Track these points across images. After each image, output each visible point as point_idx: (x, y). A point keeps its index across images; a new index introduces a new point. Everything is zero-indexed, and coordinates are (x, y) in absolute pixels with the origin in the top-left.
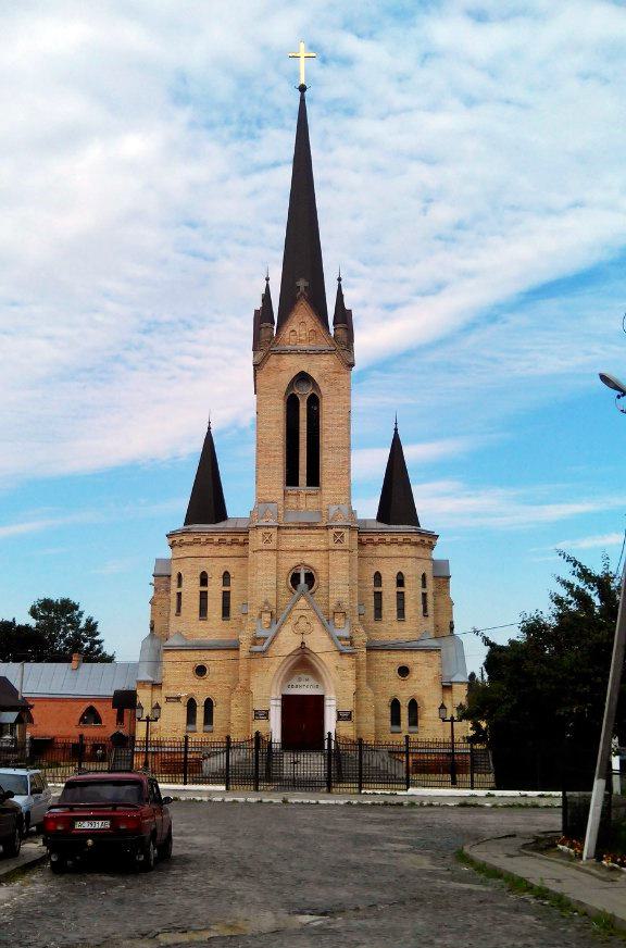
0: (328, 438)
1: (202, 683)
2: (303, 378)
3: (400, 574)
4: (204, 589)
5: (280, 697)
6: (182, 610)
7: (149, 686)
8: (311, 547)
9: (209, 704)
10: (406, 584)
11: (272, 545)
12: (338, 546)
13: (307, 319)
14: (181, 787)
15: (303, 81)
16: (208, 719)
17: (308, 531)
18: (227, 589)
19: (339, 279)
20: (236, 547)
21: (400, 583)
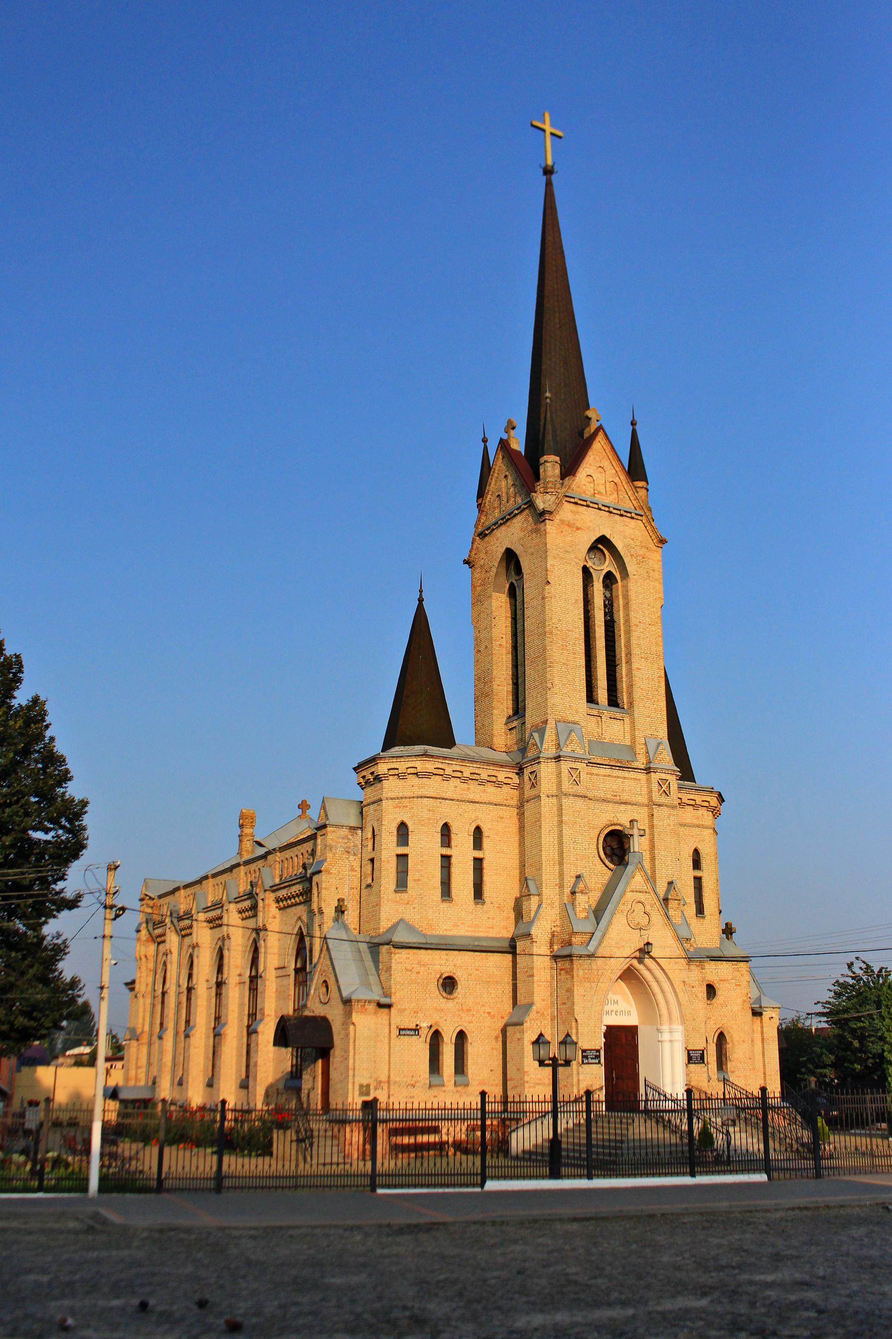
0: (639, 637)
1: (450, 1005)
2: (602, 545)
3: (696, 852)
4: (446, 851)
5: (605, 1027)
6: (410, 884)
7: (372, 1007)
8: (625, 797)
9: (461, 1036)
10: (704, 863)
11: (580, 790)
12: (663, 800)
13: (606, 464)
14: (687, 1180)
15: (550, 162)
16: (460, 1067)
17: (620, 773)
18: (479, 854)
19: (633, 423)
20: (490, 788)
21: (697, 864)
